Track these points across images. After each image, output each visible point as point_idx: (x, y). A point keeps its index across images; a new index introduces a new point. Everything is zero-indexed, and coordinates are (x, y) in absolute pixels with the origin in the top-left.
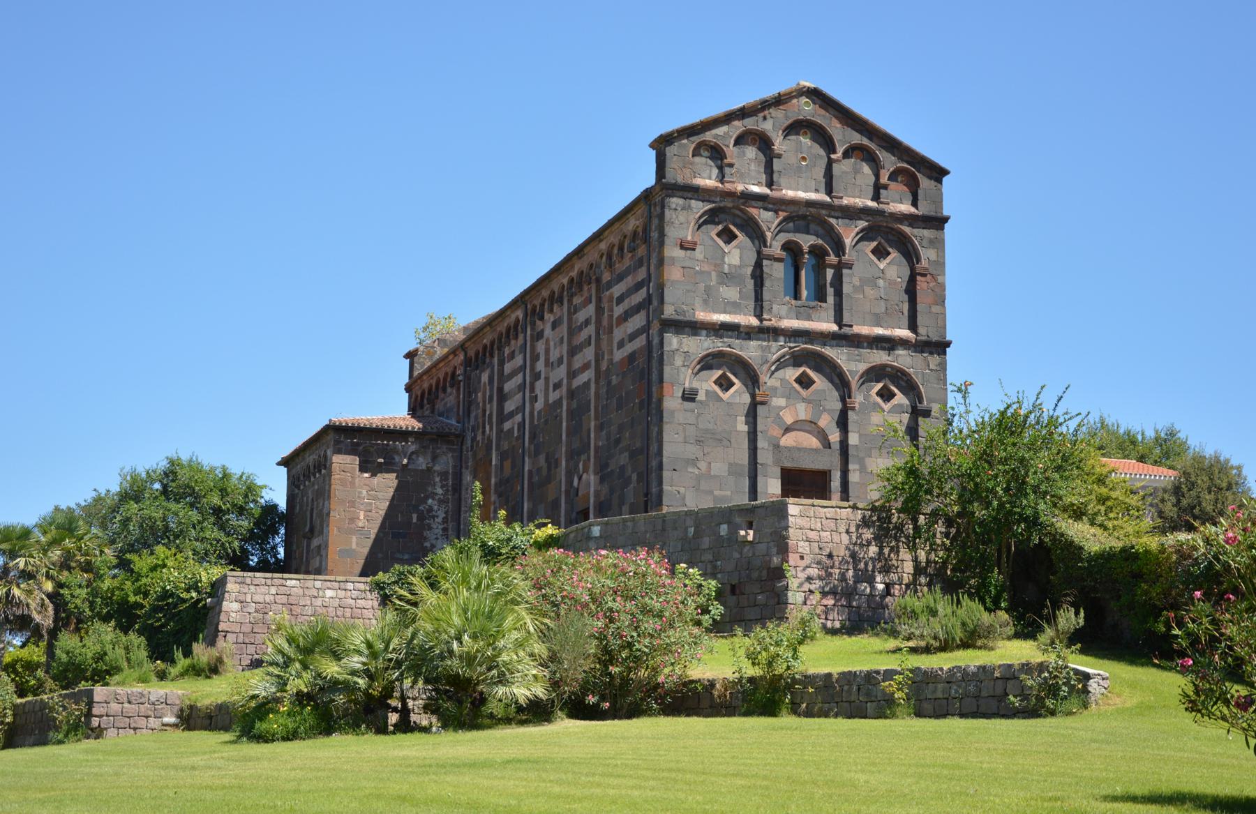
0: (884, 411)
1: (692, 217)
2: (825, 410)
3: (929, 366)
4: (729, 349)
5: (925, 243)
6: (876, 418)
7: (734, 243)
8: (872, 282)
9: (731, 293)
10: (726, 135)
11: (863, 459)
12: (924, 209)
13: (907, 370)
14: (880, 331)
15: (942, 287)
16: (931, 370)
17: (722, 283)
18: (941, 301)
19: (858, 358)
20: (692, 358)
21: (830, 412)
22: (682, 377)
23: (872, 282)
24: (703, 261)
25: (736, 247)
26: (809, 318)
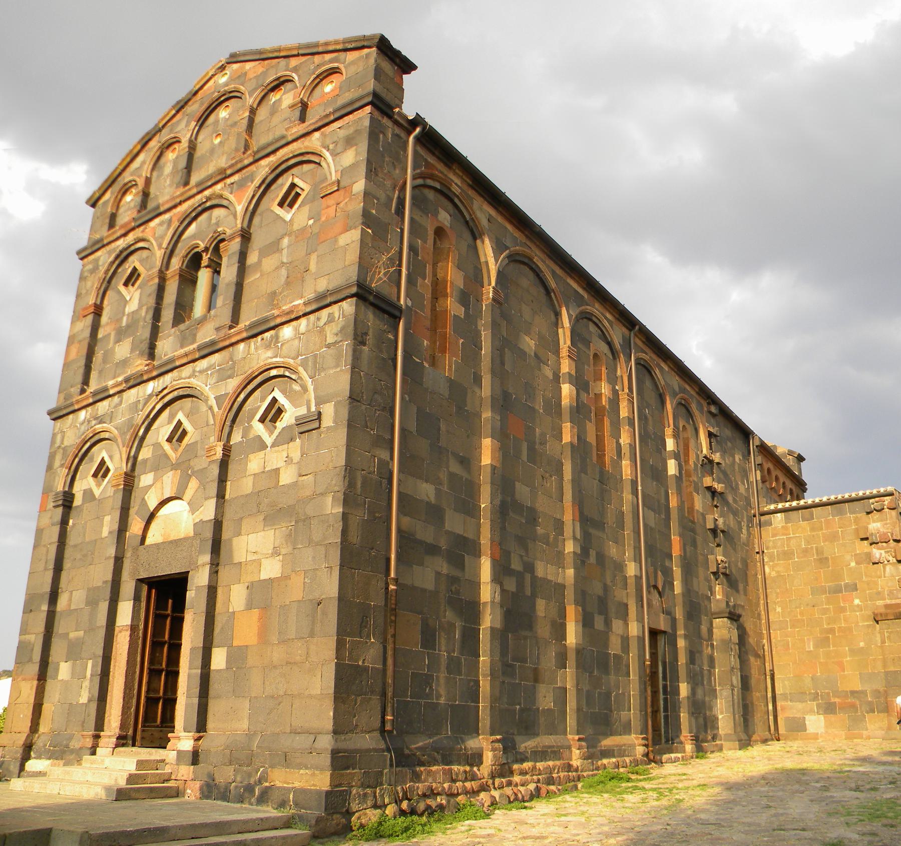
0: (263, 446)
1: (97, 277)
2: (193, 473)
4: (100, 426)
11: (230, 540)
13: (291, 361)
16: (328, 346)
17: (118, 341)
21: (200, 474)
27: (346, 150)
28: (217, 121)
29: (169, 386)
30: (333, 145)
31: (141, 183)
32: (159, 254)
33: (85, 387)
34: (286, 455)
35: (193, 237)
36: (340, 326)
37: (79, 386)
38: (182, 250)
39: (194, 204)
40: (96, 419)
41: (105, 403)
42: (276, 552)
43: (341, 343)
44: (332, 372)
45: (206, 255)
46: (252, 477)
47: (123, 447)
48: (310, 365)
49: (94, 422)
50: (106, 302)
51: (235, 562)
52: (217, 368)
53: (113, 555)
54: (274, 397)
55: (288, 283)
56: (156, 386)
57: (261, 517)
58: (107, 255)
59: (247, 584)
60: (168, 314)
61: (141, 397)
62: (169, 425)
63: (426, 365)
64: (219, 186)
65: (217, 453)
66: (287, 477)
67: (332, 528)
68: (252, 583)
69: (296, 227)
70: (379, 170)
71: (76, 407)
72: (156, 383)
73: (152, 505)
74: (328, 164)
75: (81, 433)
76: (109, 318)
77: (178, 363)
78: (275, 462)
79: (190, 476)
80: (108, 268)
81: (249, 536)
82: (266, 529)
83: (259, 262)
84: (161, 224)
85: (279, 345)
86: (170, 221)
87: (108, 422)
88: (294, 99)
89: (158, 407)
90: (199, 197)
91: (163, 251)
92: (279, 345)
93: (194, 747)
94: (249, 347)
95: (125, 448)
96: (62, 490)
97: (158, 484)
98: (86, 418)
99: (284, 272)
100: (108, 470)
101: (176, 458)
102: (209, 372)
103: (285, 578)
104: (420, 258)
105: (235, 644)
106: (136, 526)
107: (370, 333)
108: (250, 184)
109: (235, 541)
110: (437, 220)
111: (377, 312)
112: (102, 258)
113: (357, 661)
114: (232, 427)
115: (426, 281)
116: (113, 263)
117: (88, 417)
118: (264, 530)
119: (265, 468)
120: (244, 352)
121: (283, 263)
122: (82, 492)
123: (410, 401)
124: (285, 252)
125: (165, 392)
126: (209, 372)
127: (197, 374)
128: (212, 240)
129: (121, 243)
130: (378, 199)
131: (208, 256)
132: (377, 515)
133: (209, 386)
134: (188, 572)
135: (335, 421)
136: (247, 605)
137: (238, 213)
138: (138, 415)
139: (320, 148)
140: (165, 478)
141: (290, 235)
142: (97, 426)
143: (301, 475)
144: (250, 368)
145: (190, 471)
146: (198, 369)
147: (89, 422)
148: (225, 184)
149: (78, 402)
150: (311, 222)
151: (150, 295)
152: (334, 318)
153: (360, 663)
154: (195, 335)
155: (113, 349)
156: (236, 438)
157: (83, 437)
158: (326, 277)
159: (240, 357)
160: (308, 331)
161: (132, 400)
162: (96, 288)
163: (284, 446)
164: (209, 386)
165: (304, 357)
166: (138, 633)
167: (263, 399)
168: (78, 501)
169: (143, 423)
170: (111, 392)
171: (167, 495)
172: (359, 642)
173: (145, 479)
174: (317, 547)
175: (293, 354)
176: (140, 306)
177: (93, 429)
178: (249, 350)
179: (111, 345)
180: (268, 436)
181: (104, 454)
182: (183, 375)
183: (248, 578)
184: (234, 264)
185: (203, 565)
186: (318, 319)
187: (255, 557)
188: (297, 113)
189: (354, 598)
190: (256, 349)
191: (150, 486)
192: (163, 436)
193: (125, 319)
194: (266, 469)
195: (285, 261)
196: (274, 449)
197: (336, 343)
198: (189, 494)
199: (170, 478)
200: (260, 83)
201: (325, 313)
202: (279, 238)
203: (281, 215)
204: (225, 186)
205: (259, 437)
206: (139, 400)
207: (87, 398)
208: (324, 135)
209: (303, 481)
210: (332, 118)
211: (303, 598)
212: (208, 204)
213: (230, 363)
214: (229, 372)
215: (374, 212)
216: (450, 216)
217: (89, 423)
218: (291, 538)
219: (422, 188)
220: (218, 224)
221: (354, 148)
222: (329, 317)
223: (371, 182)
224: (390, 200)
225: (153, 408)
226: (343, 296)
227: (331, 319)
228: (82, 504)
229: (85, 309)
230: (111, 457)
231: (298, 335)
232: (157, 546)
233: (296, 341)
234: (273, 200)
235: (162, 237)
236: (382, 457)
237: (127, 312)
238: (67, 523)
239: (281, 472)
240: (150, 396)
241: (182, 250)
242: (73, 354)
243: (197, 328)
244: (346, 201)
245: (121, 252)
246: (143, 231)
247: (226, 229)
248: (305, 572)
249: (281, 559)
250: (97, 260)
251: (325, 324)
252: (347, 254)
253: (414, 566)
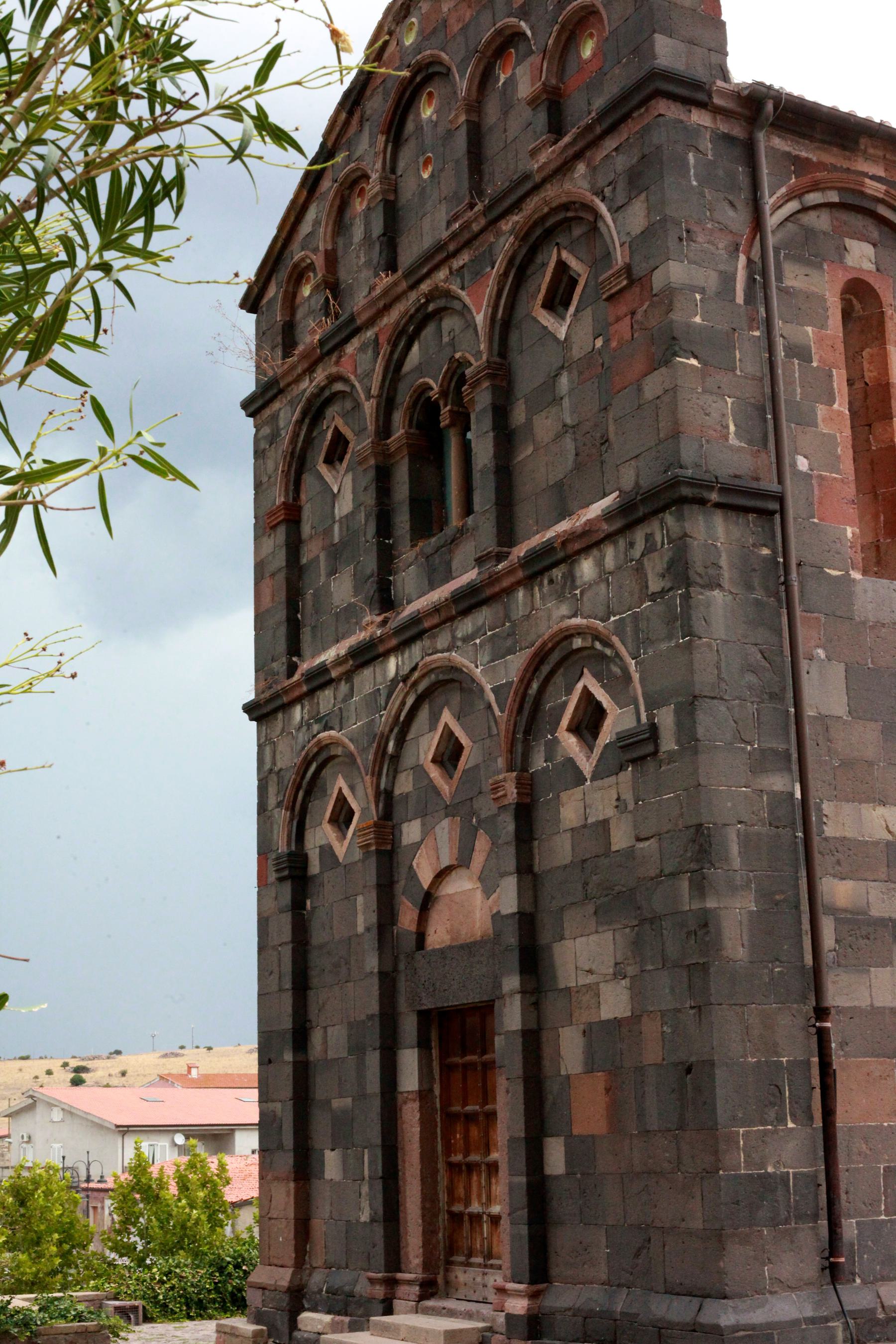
0: (580, 779)
1: (280, 452)
3: (647, 587)
11: (549, 947)
16: (653, 597)
17: (333, 572)
19: (509, 643)
20: (286, 782)
24: (311, 537)
27: (630, 199)
28: (419, 128)
29: (421, 664)
30: (610, 188)
31: (319, 261)
32: (369, 407)
33: (295, 659)
34: (615, 797)
35: (419, 369)
36: (666, 559)
37: (284, 660)
38: (404, 397)
39: (407, 312)
40: (318, 721)
41: (328, 693)
42: (618, 974)
43: (671, 593)
44: (664, 646)
45: (446, 405)
46: (569, 835)
47: (367, 775)
48: (629, 633)
49: (316, 728)
50: (303, 497)
51: (562, 986)
52: (489, 633)
53: (376, 970)
54: (585, 687)
55: (578, 467)
56: (400, 663)
57: (591, 908)
58: (288, 408)
59: (582, 1027)
60: (402, 521)
61: (381, 684)
62: (431, 734)
63: (856, 575)
64: (442, 274)
65: (509, 794)
67: (693, 937)
68: (590, 1025)
69: (577, 352)
70: (695, 229)
71: (285, 699)
72: (400, 659)
73: (426, 877)
74: (608, 226)
75: (299, 747)
76: (313, 528)
77: (427, 624)
78: (601, 807)
79: (476, 830)
80: (294, 432)
81: (578, 940)
82: (600, 929)
83: (529, 421)
84: (362, 349)
85: (578, 592)
87: (337, 727)
88: (533, 85)
89: (410, 701)
90: (413, 296)
91: (373, 402)
92: (578, 592)
93: (528, 1309)
94: (532, 595)
95: (369, 777)
96: (285, 850)
97: (429, 841)
98: (302, 718)
99: (568, 443)
100: (351, 813)
101: (451, 794)
102: (478, 641)
103: (635, 1019)
104: (815, 364)
105: (576, 1131)
106: (407, 918)
107: (724, 562)
108: (489, 269)
110: (846, 268)
111: (732, 515)
112: (282, 414)
113: (763, 1166)
114: (526, 741)
115: (836, 406)
116: (300, 422)
117: (306, 717)
118: (597, 932)
119: (586, 819)
120: (525, 604)
121: (565, 425)
122: (317, 850)
123: (829, 658)
124: (566, 402)
125: (416, 675)
126: (478, 641)
127: (459, 643)
128: (449, 375)
129: (307, 387)
130: (702, 291)
131: (448, 408)
132: (777, 897)
133: (479, 670)
134: (494, 1001)
135: (678, 742)
136: (586, 1064)
137: (479, 328)
138: (381, 716)
139: (588, 194)
140: (437, 829)
141: (569, 369)
142: (322, 735)
143: (639, 839)
144: (539, 637)
145: (474, 820)
146: (459, 635)
147: (309, 726)
148: (450, 269)
149: (286, 691)
150: (599, 343)
151: (366, 489)
152: (654, 544)
153: (770, 1170)
154: (449, 564)
155: (327, 585)
156: (539, 762)
157: (303, 753)
158: (632, 462)
159: (521, 613)
160: (619, 568)
161: (368, 689)
162: (283, 471)
163: (610, 778)
164: (480, 668)
165: (617, 617)
166: (434, 1103)
167: (569, 691)
168: (315, 867)
169: (391, 731)
170: (334, 674)
171: (445, 862)
172: (765, 1132)
173: (411, 832)
174: (676, 969)
175: (601, 611)
176: (357, 506)
177: (315, 740)
178: (532, 602)
179: (323, 579)
180: (585, 759)
181: (341, 783)
182: (439, 646)
183: (584, 1017)
184: (487, 432)
185: (512, 994)
186: (632, 545)
187: (589, 979)
188: (542, 118)
189: (745, 1056)
190: (543, 598)
192: (426, 754)
193: (336, 527)
194: (590, 821)
195: (569, 421)
196: (596, 783)
197: (663, 592)
198: (478, 859)
199: (446, 830)
200: (472, 47)
201: (639, 536)
202: (553, 374)
203: (550, 328)
204: (451, 273)
205: (570, 762)
206: (379, 690)
207: (298, 684)
208: (593, 170)
209: (641, 848)
210: (598, 130)
211: (664, 1059)
212: (431, 308)
213: (507, 624)
214: (509, 643)
215: (698, 319)
216: (874, 245)
217: (308, 729)
218: (637, 944)
219: (799, 216)
220: (452, 344)
221: (644, 195)
222: (647, 541)
223: (682, 262)
224: (728, 279)
225: (403, 703)
226: (662, 503)
228: (321, 872)
229: (271, 514)
230: (352, 788)
231: (603, 576)
232: (442, 952)
233: (603, 586)
234: (534, 297)
235: (369, 374)
236: (775, 788)
237: (337, 518)
238: (304, 907)
239: (611, 826)
240: (394, 682)
241: (404, 397)
242: (267, 602)
243: (450, 552)
244: (645, 307)
245: (309, 401)
246: (337, 363)
247: (467, 355)
248: (663, 1013)
249: (628, 985)
251: (643, 555)
252: (660, 419)
253: (872, 969)
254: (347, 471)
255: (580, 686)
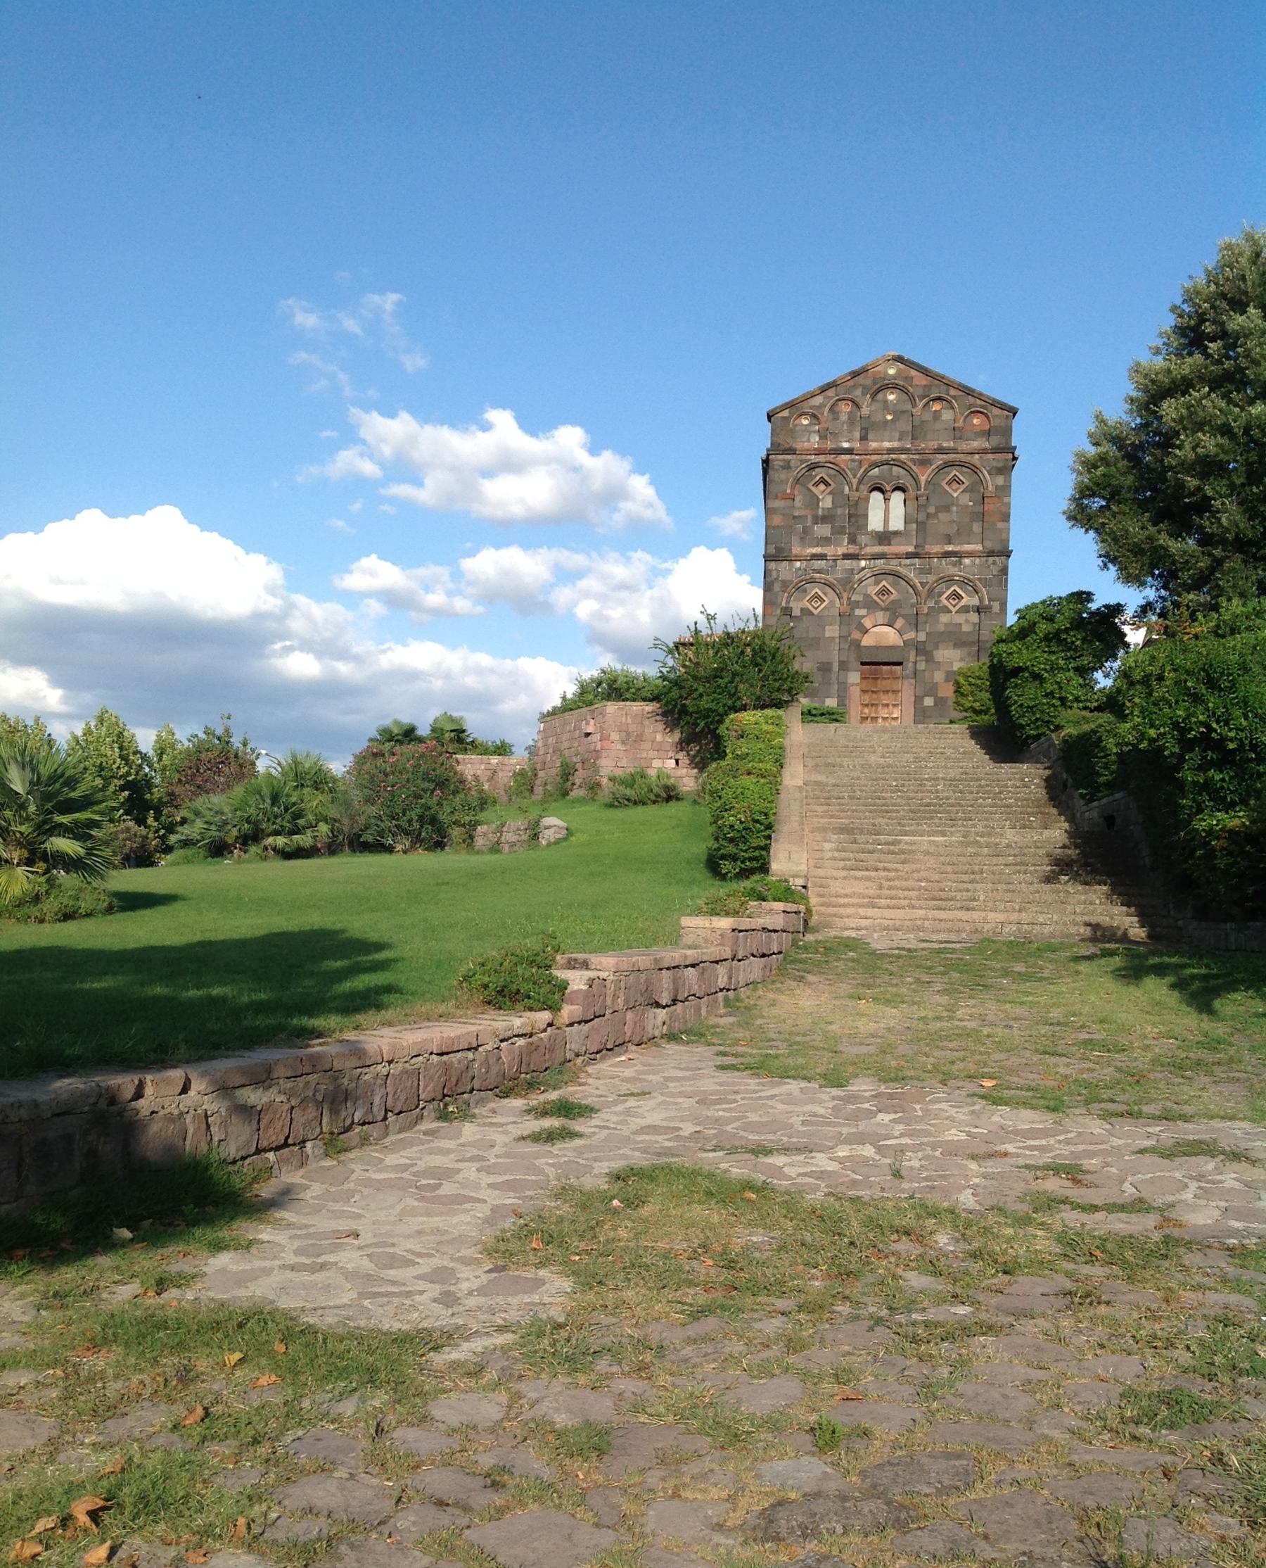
5: (993, 472)
6: (944, 618)
7: (829, 490)
8: (947, 509)
9: (823, 530)
10: (822, 406)
12: (996, 440)
14: (950, 548)
15: (1009, 504)
17: (817, 523)
18: (1006, 517)
22: (779, 599)
23: (947, 509)
25: (829, 493)
26: (889, 544)
42: (962, 660)
57: (952, 643)
66: (966, 628)
86: (860, 462)
109: (935, 652)
141: (957, 505)
167: (948, 588)
191: (864, 616)
201: (991, 559)
205: (947, 607)
227: (994, 563)
240: (864, 569)
250: (789, 461)
254: (829, 493)
255: (952, 589)
